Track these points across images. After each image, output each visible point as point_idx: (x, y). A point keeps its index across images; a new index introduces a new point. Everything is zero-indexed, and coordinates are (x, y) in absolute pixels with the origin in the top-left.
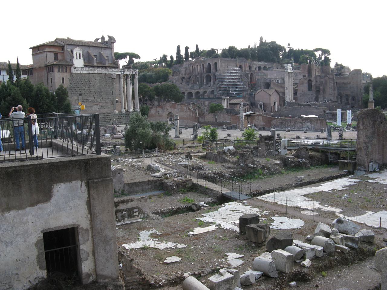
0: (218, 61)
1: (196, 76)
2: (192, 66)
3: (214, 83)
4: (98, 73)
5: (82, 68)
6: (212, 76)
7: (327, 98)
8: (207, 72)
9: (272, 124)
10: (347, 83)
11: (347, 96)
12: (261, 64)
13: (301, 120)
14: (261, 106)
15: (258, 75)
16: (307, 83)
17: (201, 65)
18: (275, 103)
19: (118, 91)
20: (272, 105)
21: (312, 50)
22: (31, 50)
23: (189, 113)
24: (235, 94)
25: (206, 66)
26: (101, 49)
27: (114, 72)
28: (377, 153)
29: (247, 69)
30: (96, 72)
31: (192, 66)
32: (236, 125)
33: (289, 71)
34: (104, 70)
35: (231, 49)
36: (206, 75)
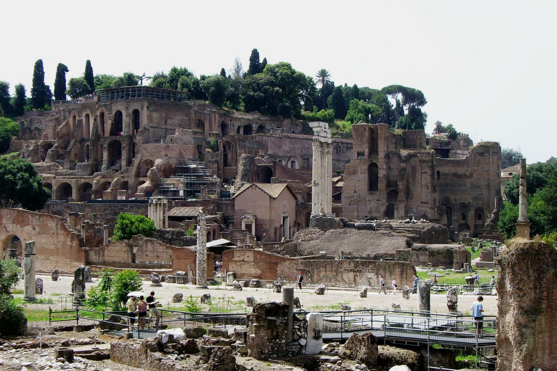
0: (142, 108)
1: (83, 141)
2: (74, 117)
9: (279, 272)
10: (465, 175)
11: (465, 207)
13: (352, 265)
14: (249, 227)
17: (98, 113)
18: (284, 218)
20: (278, 225)
21: (380, 89)
23: (62, 238)
28: (547, 351)
31: (74, 117)
32: (186, 274)
33: (323, 140)
36: (109, 140)
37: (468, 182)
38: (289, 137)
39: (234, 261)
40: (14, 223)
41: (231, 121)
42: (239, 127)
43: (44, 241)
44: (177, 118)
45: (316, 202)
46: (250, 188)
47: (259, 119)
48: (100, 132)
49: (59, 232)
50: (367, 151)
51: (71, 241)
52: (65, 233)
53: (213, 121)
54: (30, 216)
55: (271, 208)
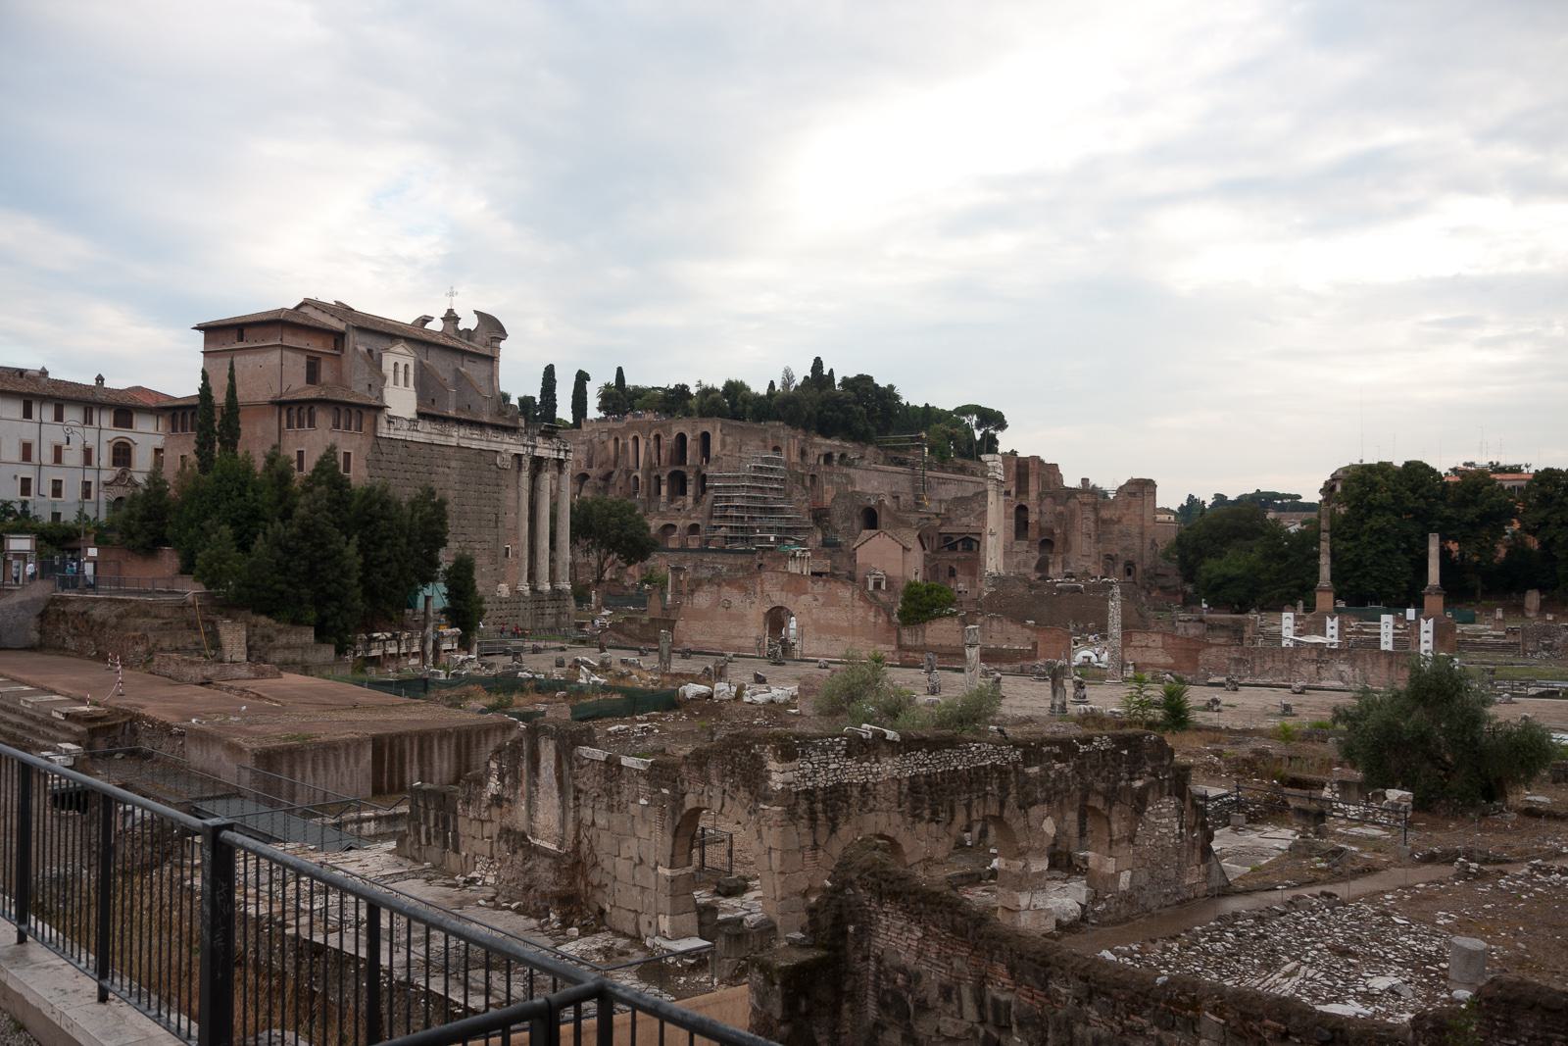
2: (617, 440)
3: (697, 500)
4: (459, 447)
5: (410, 420)
6: (690, 477)
7: (1073, 565)
8: (672, 462)
12: (833, 444)
15: (831, 482)
16: (1014, 516)
17: (652, 437)
22: (201, 335)
23: (860, 612)
24: (772, 539)
25: (668, 440)
26: (459, 357)
27: (505, 446)
29: (795, 458)
30: (453, 442)
31: (617, 440)
34: (476, 433)
35: (734, 389)
36: (669, 471)
44: (870, 450)
48: (655, 460)
49: (857, 604)
52: (867, 605)
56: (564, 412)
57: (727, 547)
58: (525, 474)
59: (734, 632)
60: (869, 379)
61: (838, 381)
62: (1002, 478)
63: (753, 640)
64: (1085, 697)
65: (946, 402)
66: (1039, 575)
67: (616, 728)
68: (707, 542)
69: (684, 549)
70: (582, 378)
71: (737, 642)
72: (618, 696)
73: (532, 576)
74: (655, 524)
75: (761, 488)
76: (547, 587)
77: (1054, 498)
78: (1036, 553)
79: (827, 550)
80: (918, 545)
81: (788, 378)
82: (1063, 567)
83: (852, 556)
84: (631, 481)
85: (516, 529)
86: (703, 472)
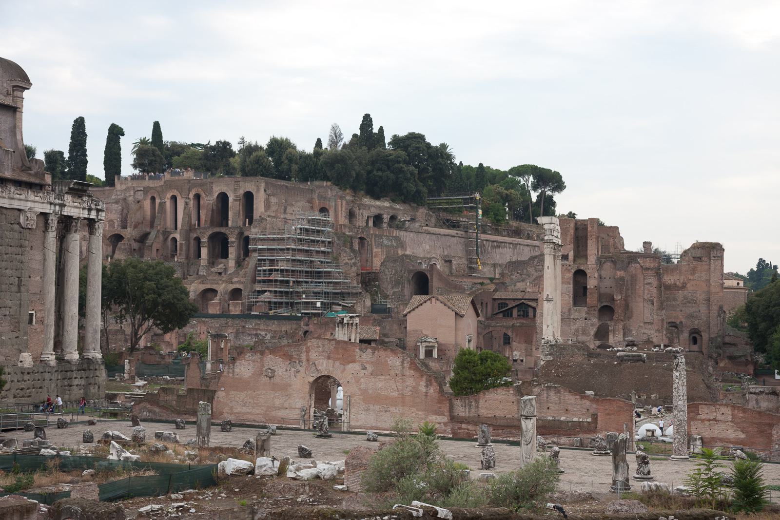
2: (153, 199)
3: (239, 264)
6: (232, 239)
8: (213, 224)
12: (383, 205)
15: (381, 245)
16: (571, 282)
17: (191, 196)
19: (38, 278)
21: (507, 170)
23: (410, 382)
24: (319, 305)
25: (209, 200)
27: (29, 204)
29: (343, 220)
31: (153, 199)
35: (279, 147)
36: (210, 232)
37: (680, 294)
38: (429, 233)
39: (700, 420)
40: (329, 358)
41: (359, 209)
42: (368, 217)
43: (380, 385)
44: (422, 212)
45: (549, 322)
46: (429, 302)
47: (391, 207)
48: (194, 221)
49: (407, 373)
50: (571, 255)
51: (427, 386)
52: (417, 374)
53: (340, 209)
54: (357, 350)
55: (456, 329)
56: (96, 168)
57: (271, 313)
58: (52, 235)
59: (277, 402)
60: (420, 138)
61: (388, 139)
62: (558, 241)
63: (298, 412)
64: (649, 473)
65: (502, 163)
66: (598, 343)
67: (148, 508)
68: (250, 308)
69: (225, 315)
70: (115, 133)
71: (282, 414)
72: (151, 473)
73: (59, 344)
74: (194, 288)
75: (307, 251)
76: (76, 356)
77: (614, 263)
78: (595, 320)
79: (376, 316)
80: (471, 311)
81: (336, 136)
82: (624, 334)
83: (403, 323)
84: (169, 242)
85: (42, 293)
86: (246, 233)
